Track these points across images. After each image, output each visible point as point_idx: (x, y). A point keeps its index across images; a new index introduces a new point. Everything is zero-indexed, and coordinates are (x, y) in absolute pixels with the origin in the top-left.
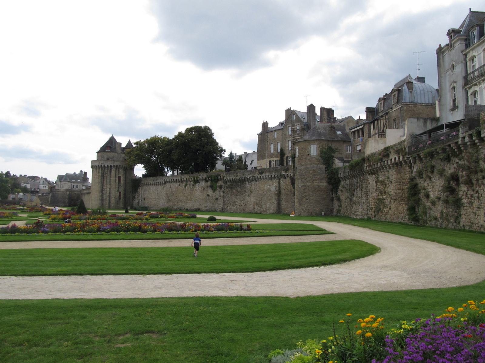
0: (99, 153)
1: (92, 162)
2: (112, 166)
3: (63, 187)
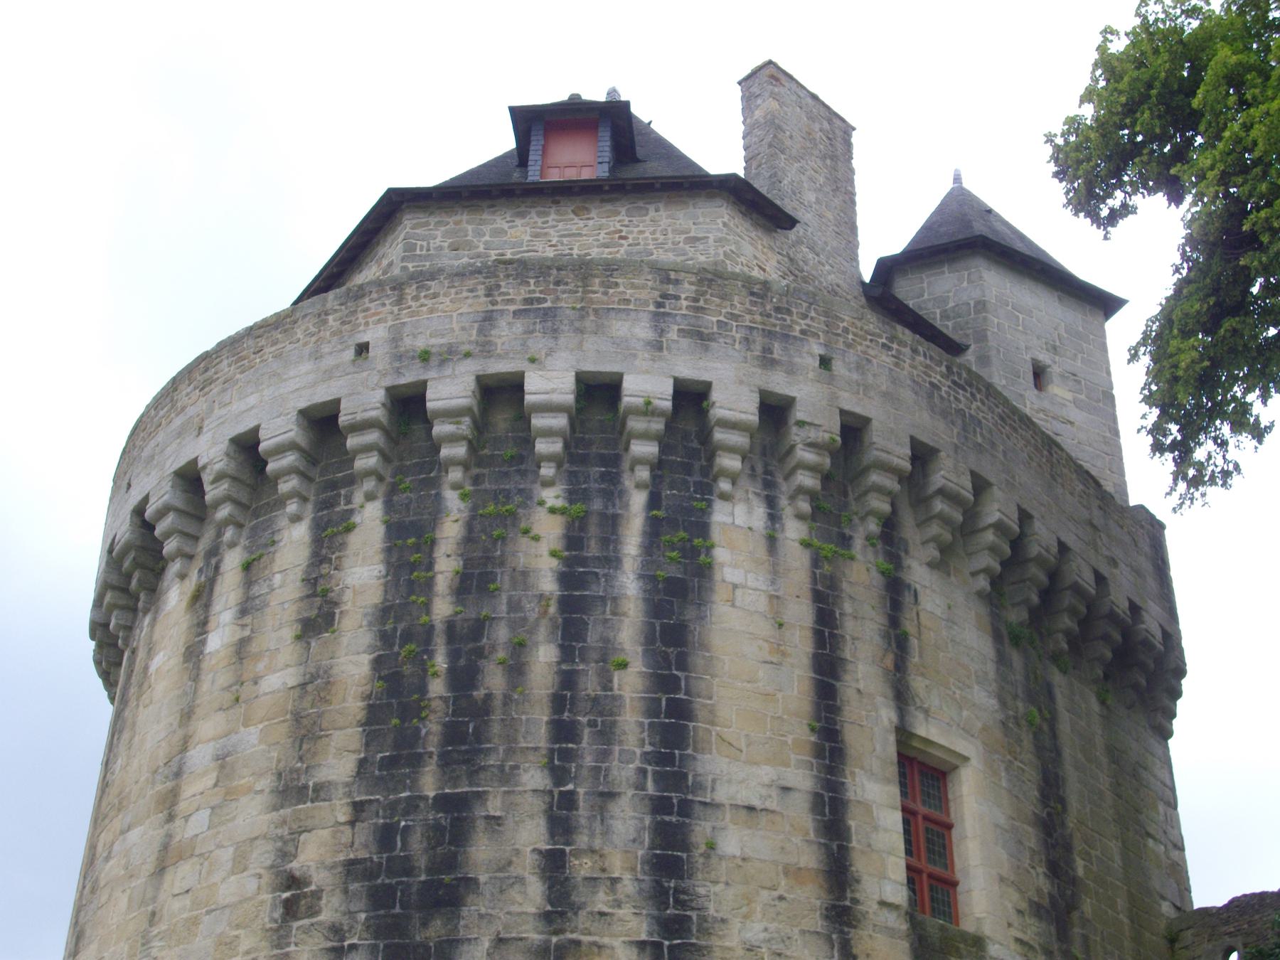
2: (734, 402)
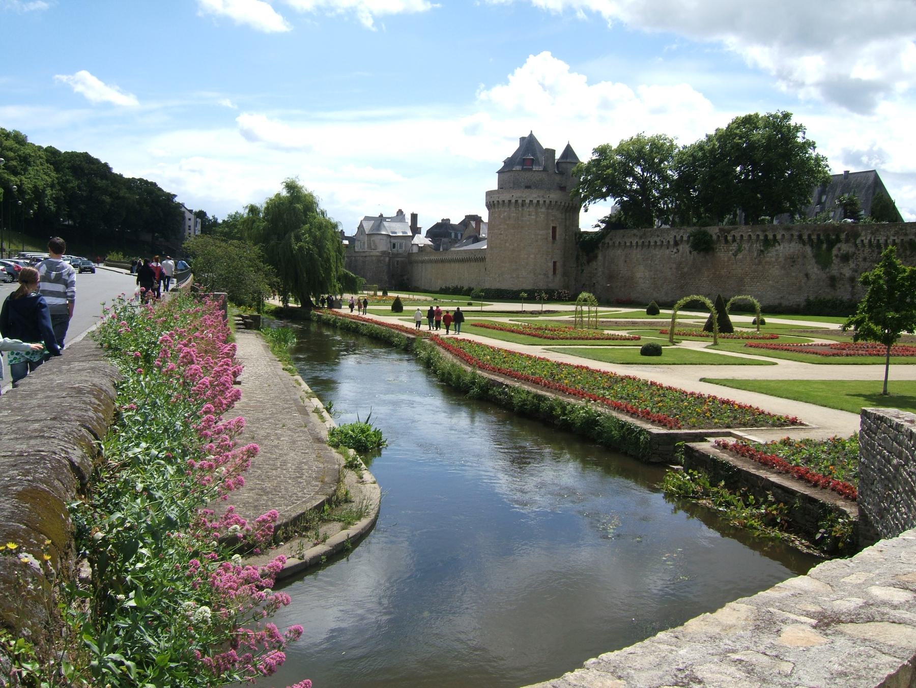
0: (506, 176)
1: (489, 194)
3: (376, 246)
